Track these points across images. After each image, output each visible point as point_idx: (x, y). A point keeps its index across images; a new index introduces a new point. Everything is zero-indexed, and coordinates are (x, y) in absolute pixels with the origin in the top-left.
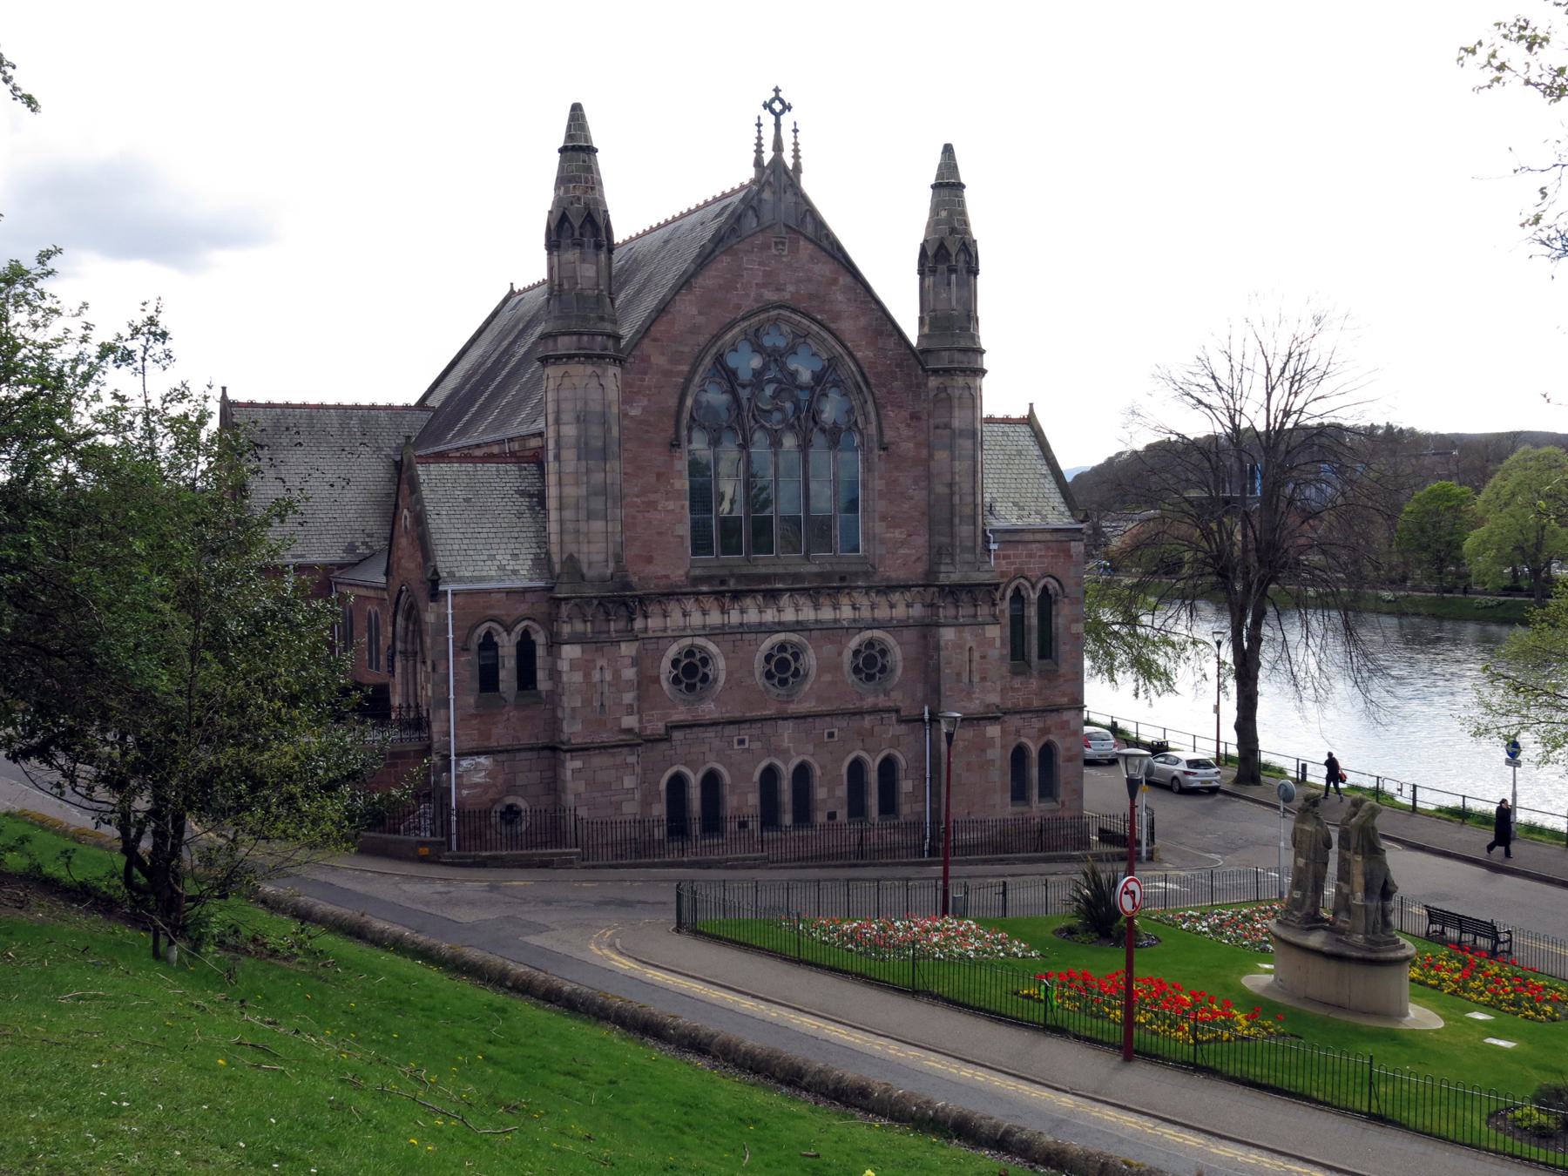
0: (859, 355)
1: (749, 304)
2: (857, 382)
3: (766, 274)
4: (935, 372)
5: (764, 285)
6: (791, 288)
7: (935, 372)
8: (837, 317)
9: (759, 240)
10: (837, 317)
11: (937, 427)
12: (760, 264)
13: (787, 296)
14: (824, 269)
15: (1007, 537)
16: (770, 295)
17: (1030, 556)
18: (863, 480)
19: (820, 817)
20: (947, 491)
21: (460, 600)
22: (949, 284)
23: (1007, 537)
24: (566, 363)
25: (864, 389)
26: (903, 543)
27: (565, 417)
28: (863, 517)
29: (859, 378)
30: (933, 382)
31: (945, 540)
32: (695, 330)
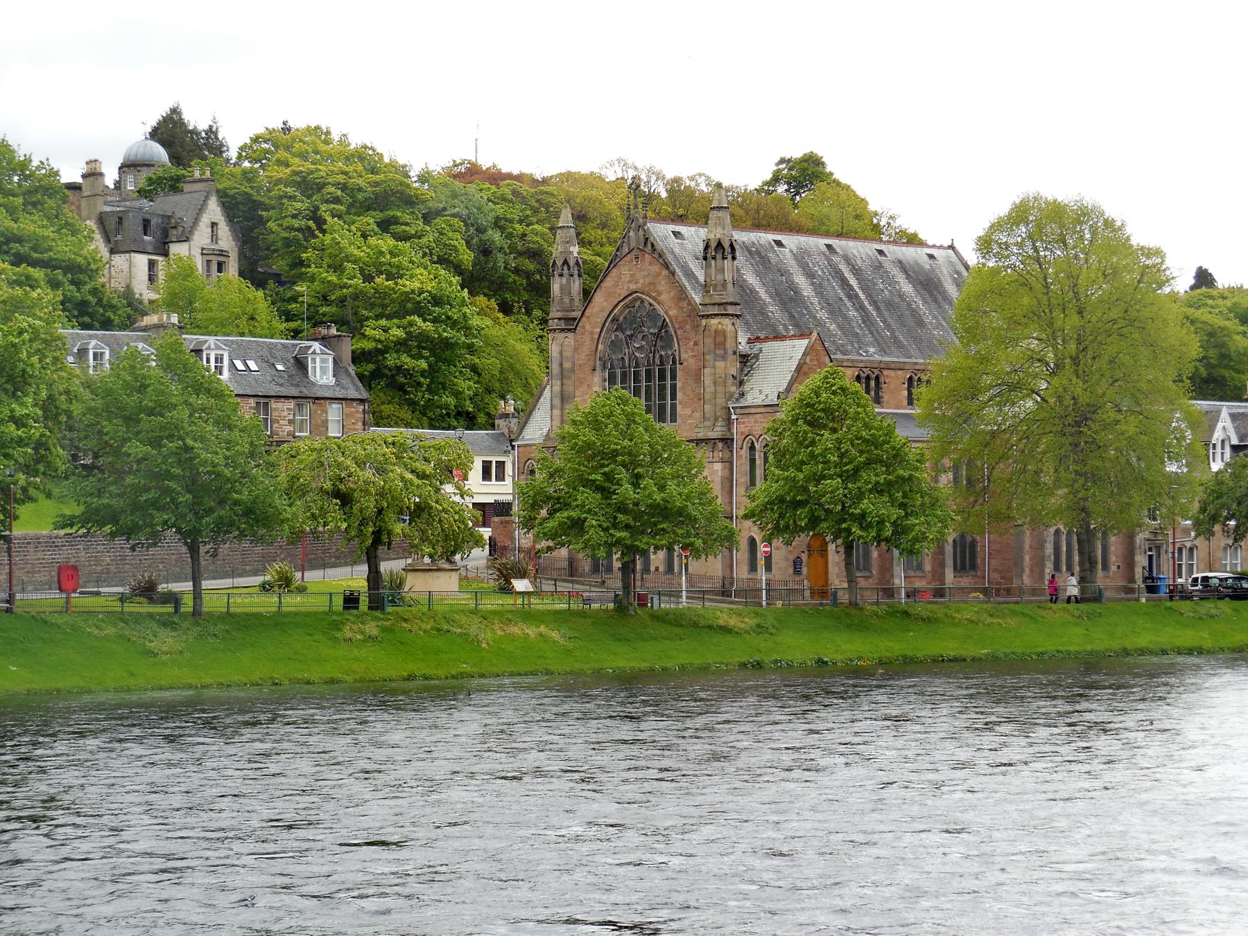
0: (671, 313)
1: (624, 293)
3: (631, 275)
5: (630, 282)
6: (641, 281)
8: (659, 294)
9: (628, 258)
10: (659, 294)
12: (629, 270)
13: (639, 285)
14: (656, 268)
15: (743, 411)
16: (633, 287)
17: (756, 422)
19: (652, 569)
21: (521, 449)
23: (743, 411)
26: (690, 416)
30: (704, 322)
32: (602, 310)
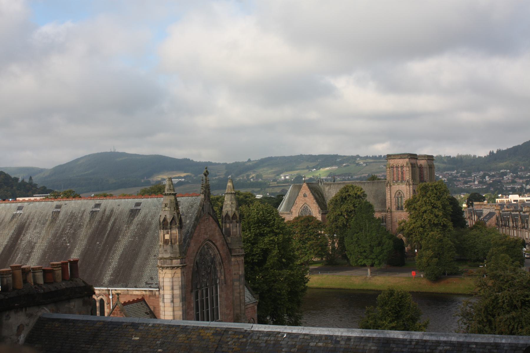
2: (220, 262)
4: (235, 256)
7: (235, 256)
11: (235, 274)
18: (220, 295)
20: (238, 295)
22: (236, 226)
24: (176, 269)
25: (222, 264)
27: (175, 287)
28: (220, 307)
29: (221, 261)
30: (233, 259)
31: (238, 312)
